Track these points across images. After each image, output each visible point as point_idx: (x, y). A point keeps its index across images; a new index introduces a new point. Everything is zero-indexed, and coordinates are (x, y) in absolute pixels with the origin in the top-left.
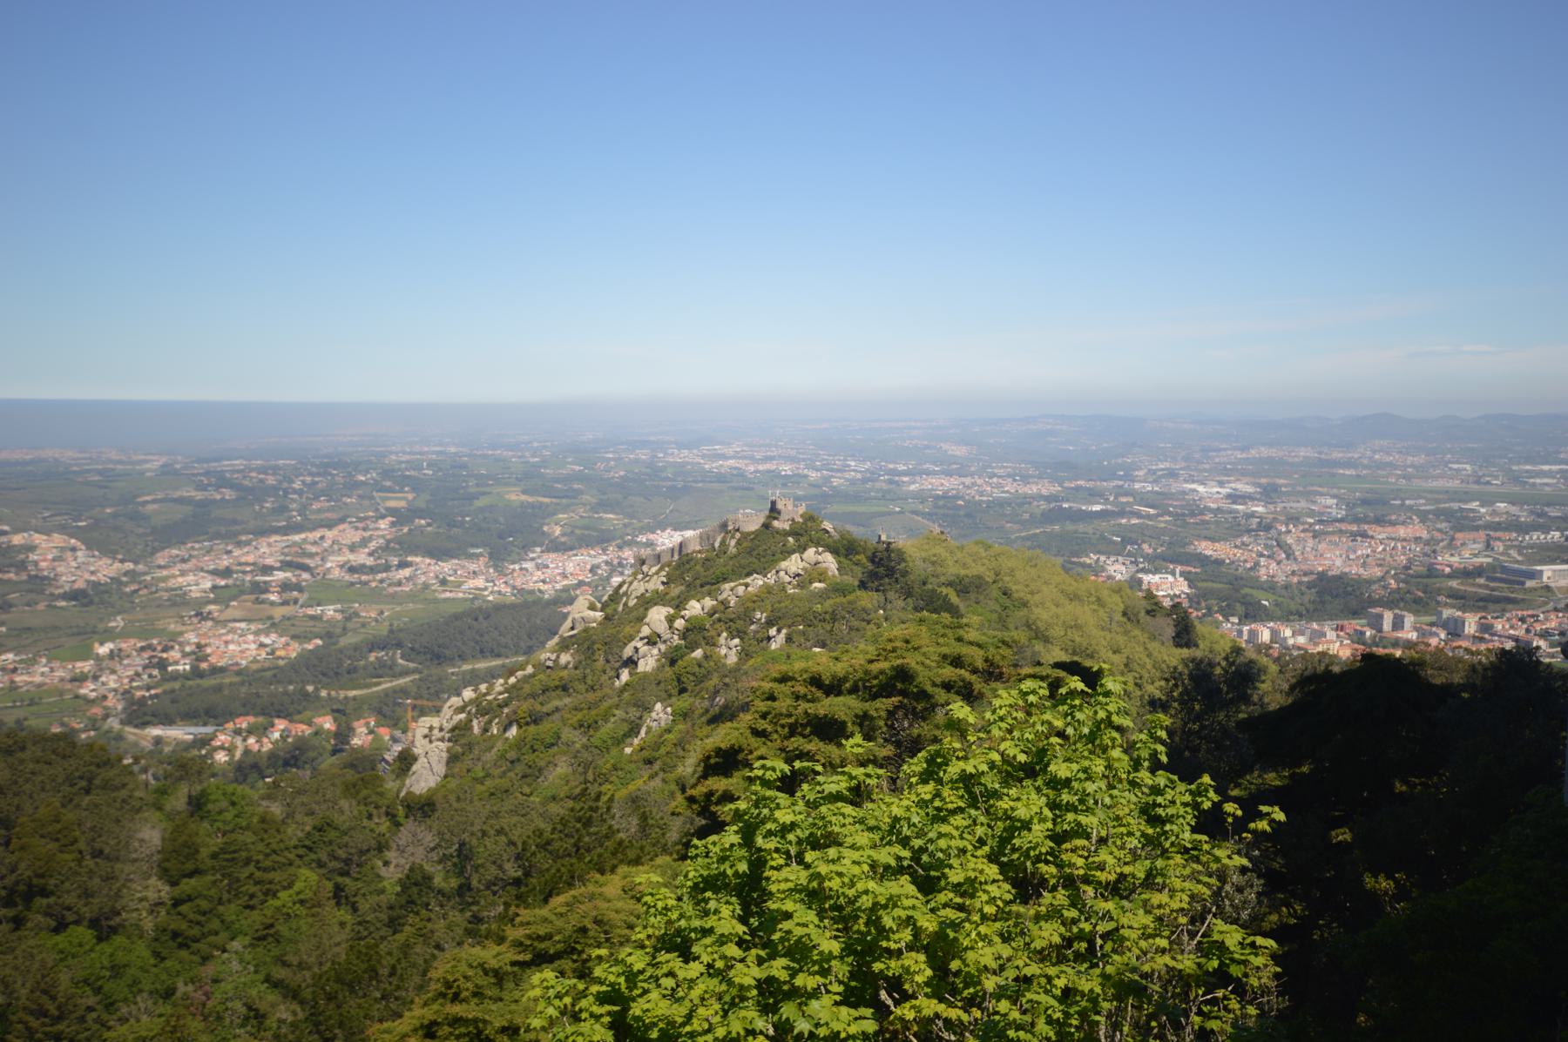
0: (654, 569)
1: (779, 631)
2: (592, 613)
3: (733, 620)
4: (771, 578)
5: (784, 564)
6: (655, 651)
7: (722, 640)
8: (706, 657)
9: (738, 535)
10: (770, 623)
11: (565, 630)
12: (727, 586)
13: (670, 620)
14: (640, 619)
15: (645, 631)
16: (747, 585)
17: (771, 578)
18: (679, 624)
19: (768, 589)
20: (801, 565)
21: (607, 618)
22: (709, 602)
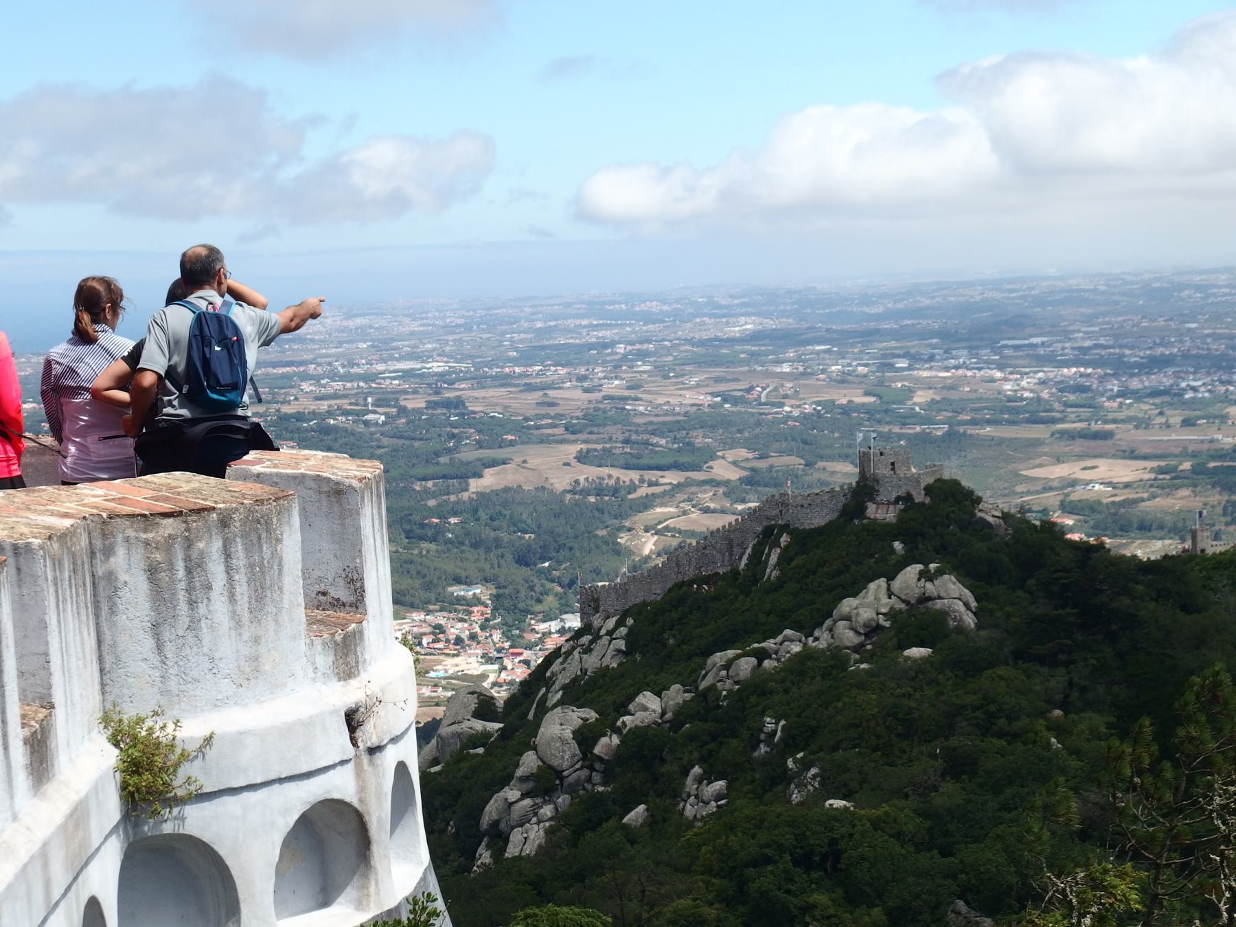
0: (611, 623)
2: (479, 725)
3: (714, 729)
4: (822, 640)
5: (848, 605)
6: (547, 811)
7: (690, 784)
8: (652, 821)
9: (785, 539)
10: (790, 744)
12: (719, 658)
13: (585, 737)
15: (529, 762)
16: (762, 655)
17: (822, 640)
18: (607, 744)
20: (886, 604)
21: (503, 733)
22: (677, 694)
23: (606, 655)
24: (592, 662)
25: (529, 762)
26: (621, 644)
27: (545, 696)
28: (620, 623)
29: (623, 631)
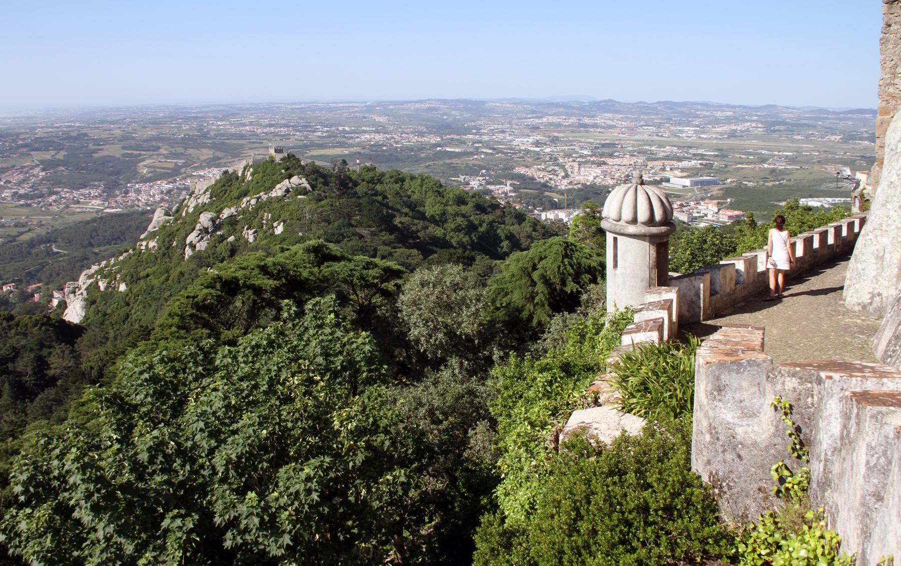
0: (202, 191)
1: (279, 224)
2: (167, 218)
5: (278, 186)
9: (251, 170)
11: (150, 228)
14: (196, 221)
19: (270, 201)
21: (176, 220)
23: (205, 199)
24: (200, 201)
25: (198, 227)
26: (208, 195)
27: (187, 211)
28: (206, 190)
29: (208, 193)
